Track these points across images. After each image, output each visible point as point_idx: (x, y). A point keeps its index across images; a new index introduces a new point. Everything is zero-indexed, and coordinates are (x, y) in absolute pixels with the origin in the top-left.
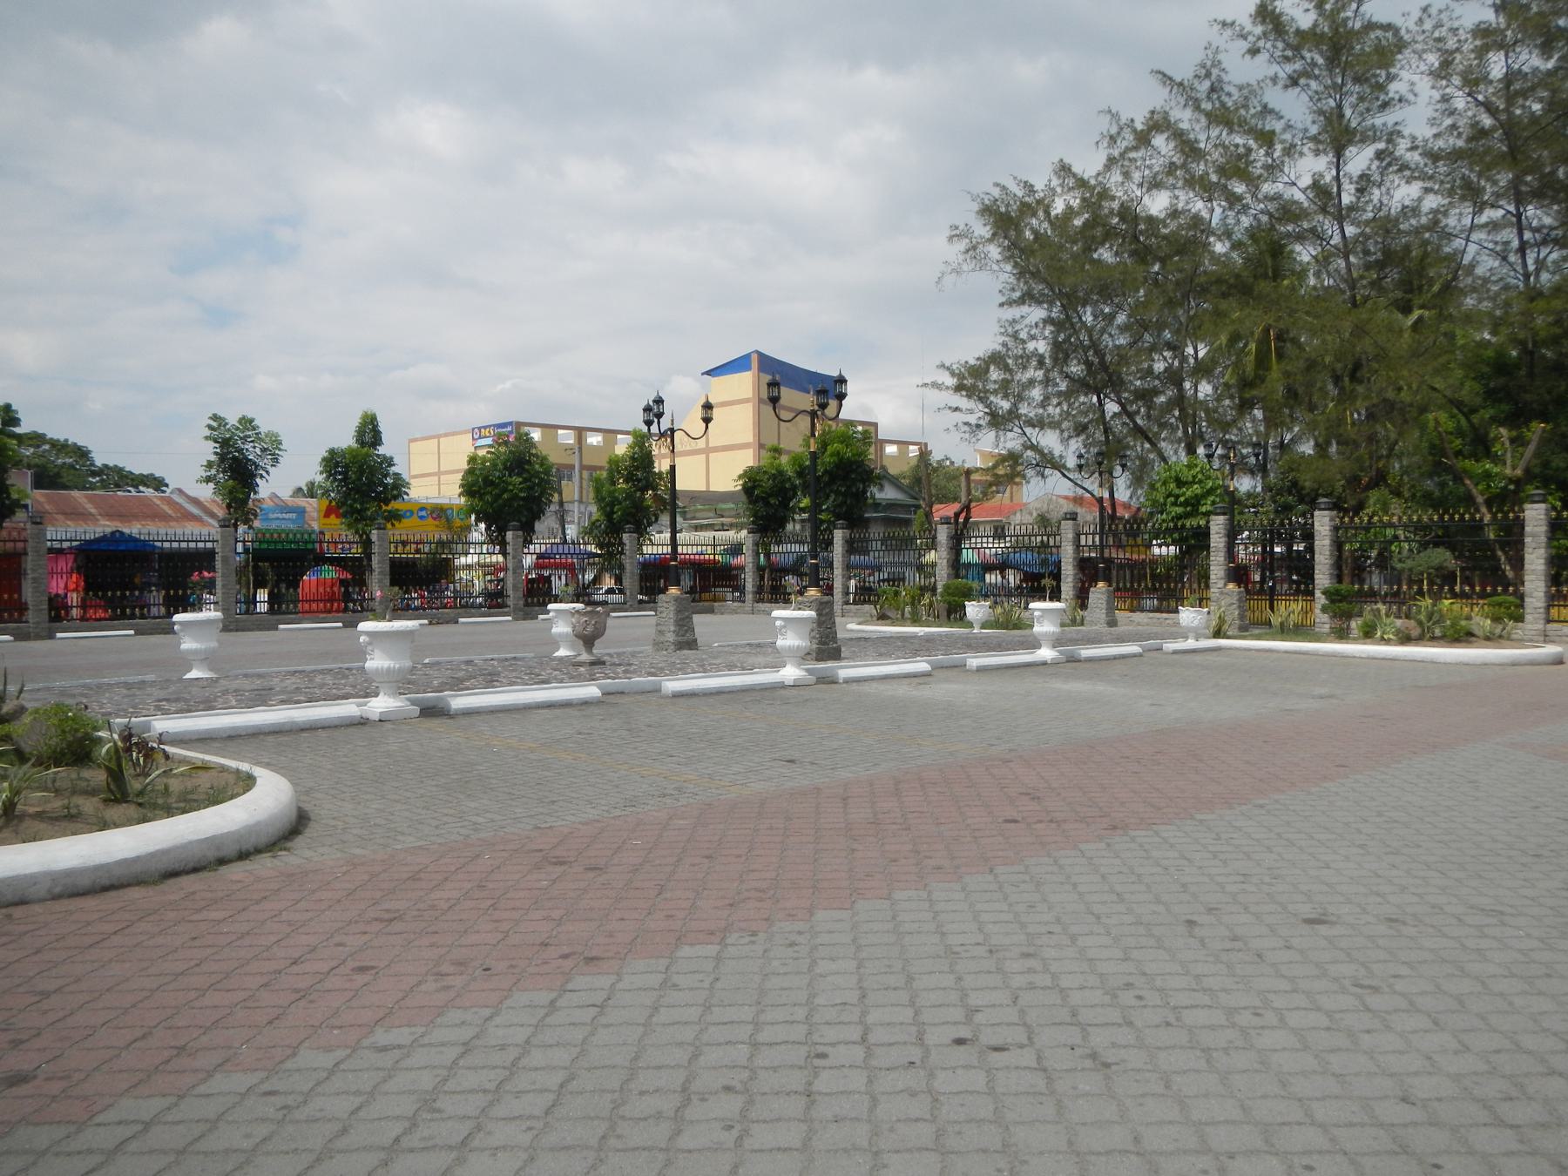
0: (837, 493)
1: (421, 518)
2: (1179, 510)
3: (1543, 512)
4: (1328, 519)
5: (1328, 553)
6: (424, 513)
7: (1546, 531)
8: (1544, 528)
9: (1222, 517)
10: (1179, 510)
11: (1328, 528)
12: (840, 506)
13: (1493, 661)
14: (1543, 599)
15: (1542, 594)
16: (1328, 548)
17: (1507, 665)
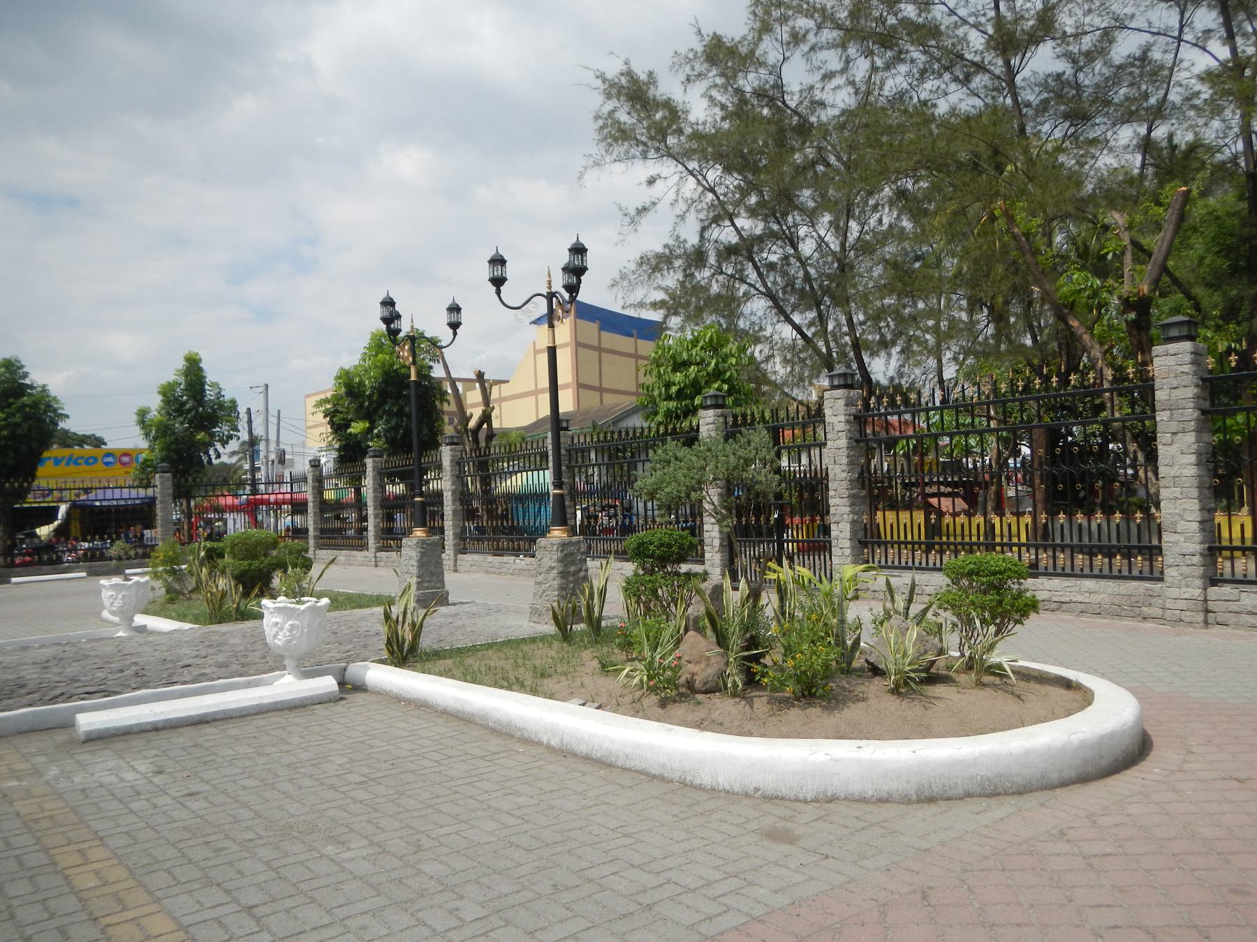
0: (389, 413)
1: (107, 464)
2: (672, 404)
3: (1188, 358)
4: (842, 402)
5: (844, 460)
6: (110, 459)
7: (1197, 397)
8: (1191, 392)
9: (711, 412)
10: (672, 404)
11: (842, 418)
12: (396, 428)
13: (856, 788)
14: (1198, 537)
15: (1195, 526)
16: (844, 452)
17: (906, 800)
